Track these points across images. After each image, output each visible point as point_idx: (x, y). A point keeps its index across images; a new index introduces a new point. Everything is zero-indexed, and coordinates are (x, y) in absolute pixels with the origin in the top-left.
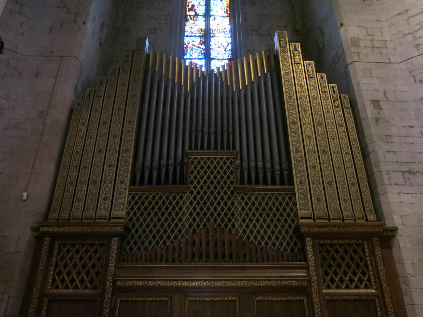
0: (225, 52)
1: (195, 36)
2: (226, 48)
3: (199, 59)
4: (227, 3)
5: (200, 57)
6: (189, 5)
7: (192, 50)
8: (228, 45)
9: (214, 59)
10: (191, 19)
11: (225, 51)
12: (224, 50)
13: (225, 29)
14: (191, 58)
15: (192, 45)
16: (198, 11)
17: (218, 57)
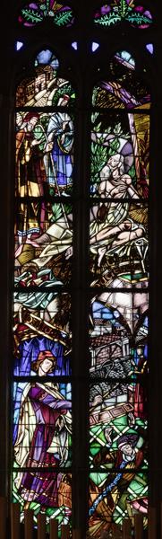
0: (126, 352)
1: (43, 289)
2: (135, 334)
3: (55, 380)
4: (141, 135)
5: (58, 373)
6: (23, 151)
7: (35, 343)
8: (140, 324)
9: (98, 380)
10: (31, 216)
11: (133, 345)
12: (127, 341)
13: (134, 252)
14: (33, 374)
15: (36, 323)
16: (51, 182)
17: (112, 374)
